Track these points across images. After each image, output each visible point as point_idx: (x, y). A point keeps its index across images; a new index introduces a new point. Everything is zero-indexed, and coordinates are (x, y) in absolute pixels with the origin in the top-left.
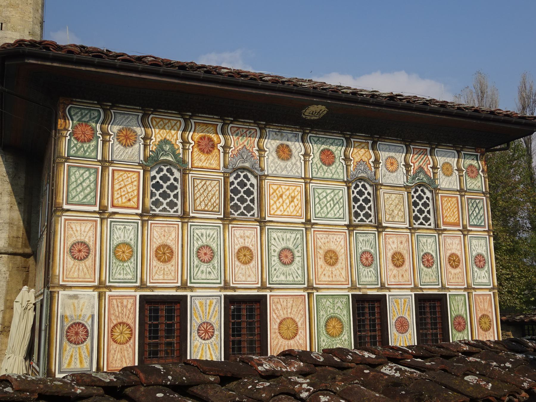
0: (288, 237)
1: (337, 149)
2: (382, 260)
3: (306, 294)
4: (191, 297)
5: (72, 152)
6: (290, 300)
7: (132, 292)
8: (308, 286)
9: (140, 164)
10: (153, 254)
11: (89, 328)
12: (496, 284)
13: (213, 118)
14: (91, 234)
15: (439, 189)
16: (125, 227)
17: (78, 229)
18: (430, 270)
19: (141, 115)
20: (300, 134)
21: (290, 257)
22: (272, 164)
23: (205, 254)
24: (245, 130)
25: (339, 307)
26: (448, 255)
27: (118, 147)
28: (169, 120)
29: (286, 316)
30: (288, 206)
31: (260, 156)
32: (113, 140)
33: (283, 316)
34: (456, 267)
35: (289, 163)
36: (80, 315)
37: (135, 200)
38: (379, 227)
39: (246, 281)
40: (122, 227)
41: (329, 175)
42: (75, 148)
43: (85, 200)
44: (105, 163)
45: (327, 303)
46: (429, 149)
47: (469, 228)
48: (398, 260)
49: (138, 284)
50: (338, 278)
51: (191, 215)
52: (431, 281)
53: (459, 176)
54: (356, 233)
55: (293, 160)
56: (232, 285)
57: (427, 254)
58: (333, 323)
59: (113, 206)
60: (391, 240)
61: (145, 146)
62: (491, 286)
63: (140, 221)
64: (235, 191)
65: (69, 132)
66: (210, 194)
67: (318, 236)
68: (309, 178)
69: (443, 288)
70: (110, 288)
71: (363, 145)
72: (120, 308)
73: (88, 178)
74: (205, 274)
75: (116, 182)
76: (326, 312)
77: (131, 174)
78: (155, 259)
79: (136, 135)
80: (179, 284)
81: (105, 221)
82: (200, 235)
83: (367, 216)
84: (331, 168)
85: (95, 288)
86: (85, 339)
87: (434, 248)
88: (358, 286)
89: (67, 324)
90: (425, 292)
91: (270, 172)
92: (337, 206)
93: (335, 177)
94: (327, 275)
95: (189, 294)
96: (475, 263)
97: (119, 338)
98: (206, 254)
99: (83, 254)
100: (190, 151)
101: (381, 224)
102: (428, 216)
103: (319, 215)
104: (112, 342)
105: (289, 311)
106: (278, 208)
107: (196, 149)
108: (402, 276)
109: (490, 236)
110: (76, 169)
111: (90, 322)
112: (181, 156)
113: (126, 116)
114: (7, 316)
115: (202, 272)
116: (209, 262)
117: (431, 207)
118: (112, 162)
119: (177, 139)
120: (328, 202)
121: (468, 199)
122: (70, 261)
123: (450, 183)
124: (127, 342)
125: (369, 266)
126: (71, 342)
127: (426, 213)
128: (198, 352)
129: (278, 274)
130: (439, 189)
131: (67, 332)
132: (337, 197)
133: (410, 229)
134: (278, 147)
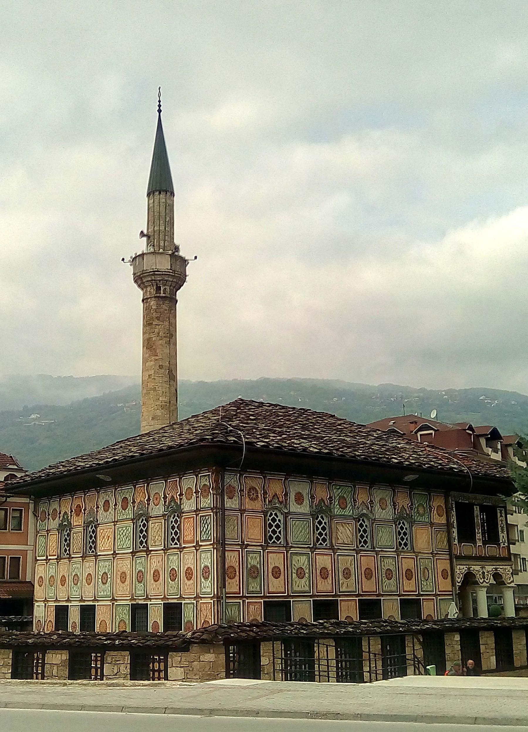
3: (111, 604)
18: (173, 583)
26: (185, 569)
31: (97, 512)
33: (101, 619)
38: (148, 551)
41: (125, 517)
45: (120, 609)
46: (178, 479)
47: (200, 544)
53: (197, 497)
58: (122, 624)
69: (181, 597)
87: (177, 564)
109: (214, 548)
121: (201, 517)
125: (141, 582)
130: (183, 513)
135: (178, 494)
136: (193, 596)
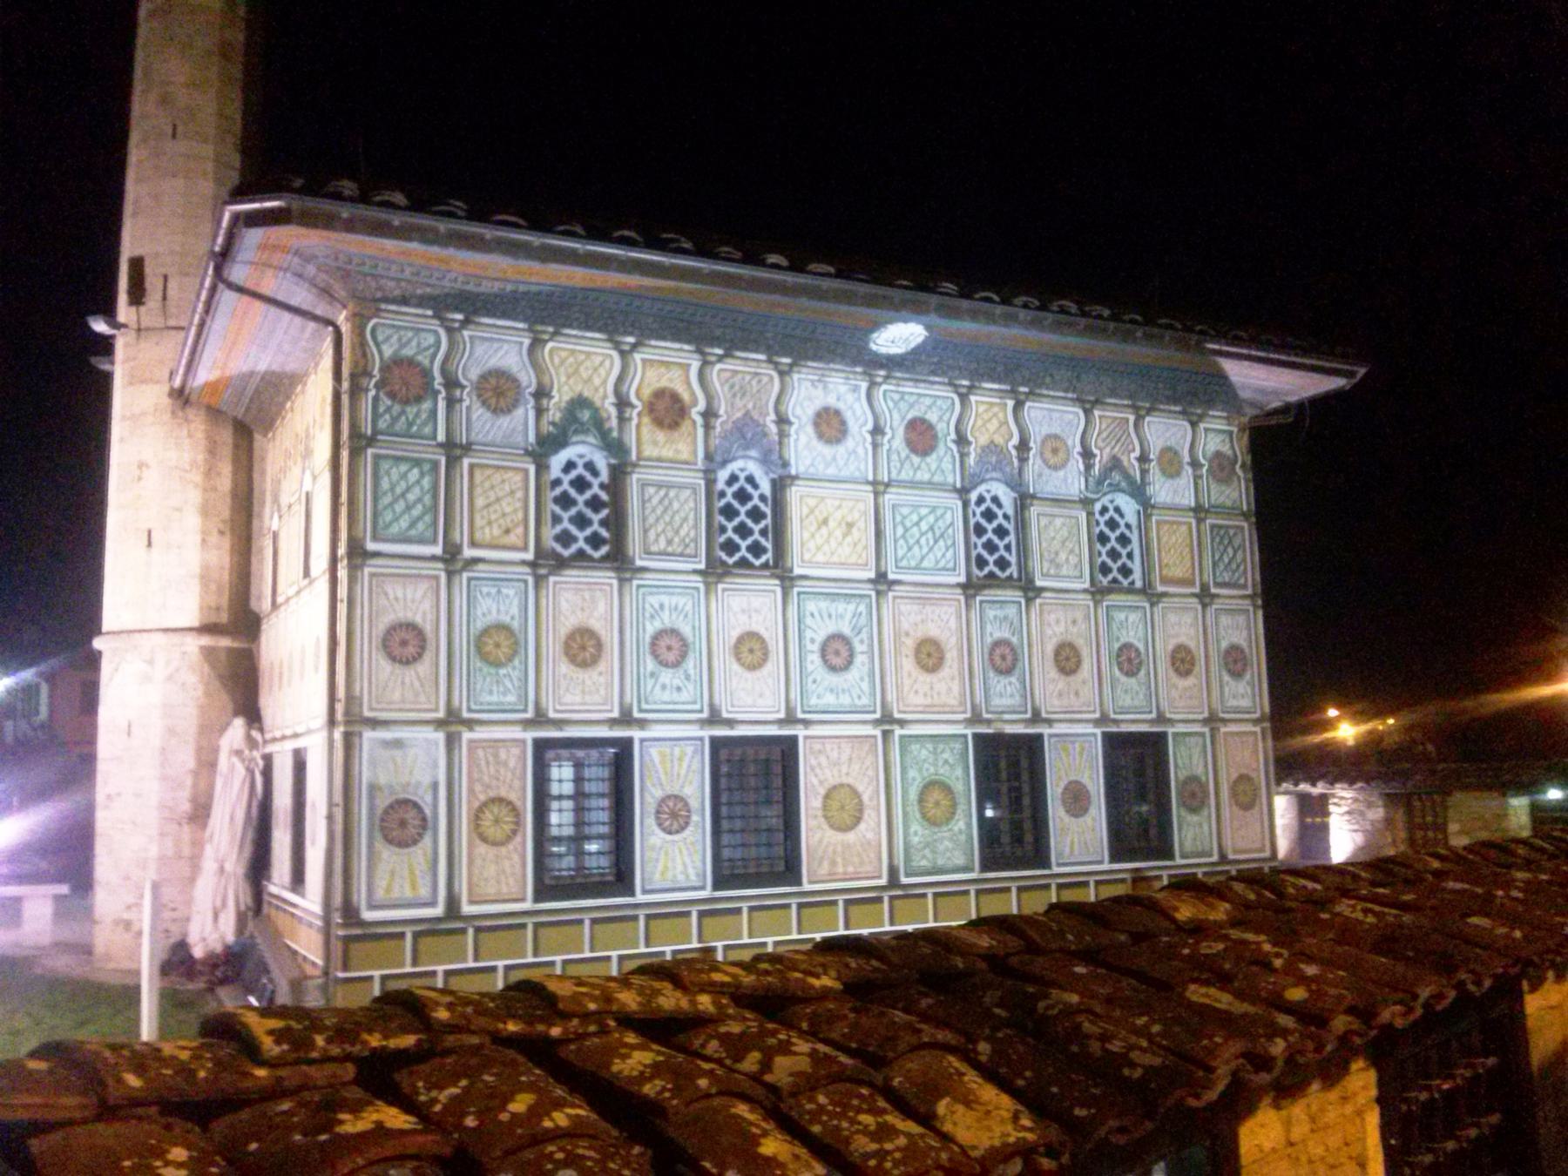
0: (841, 610)
1: (941, 418)
2: (1035, 659)
3: (877, 732)
4: (642, 740)
5: (382, 425)
6: (847, 749)
7: (516, 733)
8: (883, 716)
9: (528, 453)
10: (559, 647)
11: (428, 811)
12: (1267, 709)
13: (681, 350)
14: (427, 605)
15: (1153, 507)
16: (499, 592)
17: (400, 594)
18: (1133, 680)
19: (527, 342)
20: (864, 385)
21: (845, 654)
22: (806, 453)
23: (669, 648)
24: (748, 378)
25: (946, 762)
26: (1170, 647)
27: (479, 412)
28: (588, 354)
29: (836, 781)
30: (840, 544)
32: (468, 399)
33: (832, 781)
34: (1188, 673)
35: (841, 450)
36: (408, 784)
37: (520, 530)
38: (1030, 590)
39: (754, 704)
40: (494, 591)
42: (387, 417)
43: (413, 532)
44: (454, 450)
45: (922, 752)
46: (1132, 418)
47: (1213, 590)
48: (1067, 659)
49: (530, 715)
50: (944, 699)
51: (639, 563)
52: (1136, 703)
53: (1197, 478)
54: (981, 602)
55: (850, 442)
56: (725, 715)
57: (1127, 647)
58: (936, 795)
59: (473, 544)
60: (1053, 616)
61: (540, 412)
62: (1257, 715)
63: (531, 580)
64: (729, 512)
65: (374, 381)
66: (677, 518)
67: (903, 608)
68: (882, 483)
69: (1161, 719)
70: (470, 724)
71: (996, 409)
72: (492, 769)
73: (418, 482)
74: (671, 691)
75: (478, 491)
76: (920, 770)
77: (510, 474)
78: (564, 659)
79: (519, 386)
80: (616, 714)
81: (456, 580)
82: (657, 606)
83: (1002, 564)
84: (928, 459)
85: (439, 724)
86: (420, 835)
87: (1141, 633)
88: (986, 716)
89: (383, 802)
90: (1125, 728)
91: (802, 469)
92: (941, 543)
93: (937, 479)
94: (921, 692)
95: (636, 734)
96: (1226, 664)
97: (492, 832)
98: (670, 648)
99: (411, 650)
100: (635, 422)
101: (1031, 581)
102: (1129, 563)
103: (904, 563)
104: (478, 842)
105: (844, 770)
106: (818, 549)
107: (646, 420)
108: (1077, 694)
109: (1255, 606)
110: (390, 462)
111: (429, 798)
112: (615, 434)
113: (496, 345)
114: (202, 785)
115: (664, 687)
116: (676, 664)
117: (1135, 545)
118: (467, 448)
119: (605, 397)
120: (922, 534)
121: (1213, 527)
122: (385, 667)
123: (1175, 492)
124: (509, 839)
125: (1008, 672)
126: (389, 841)
127: (1124, 559)
128: (657, 860)
129: (820, 690)
131: (382, 820)
132: (940, 523)
133: (1093, 594)
134: (818, 415)
135: (1133, 455)
136: (1200, 717)
